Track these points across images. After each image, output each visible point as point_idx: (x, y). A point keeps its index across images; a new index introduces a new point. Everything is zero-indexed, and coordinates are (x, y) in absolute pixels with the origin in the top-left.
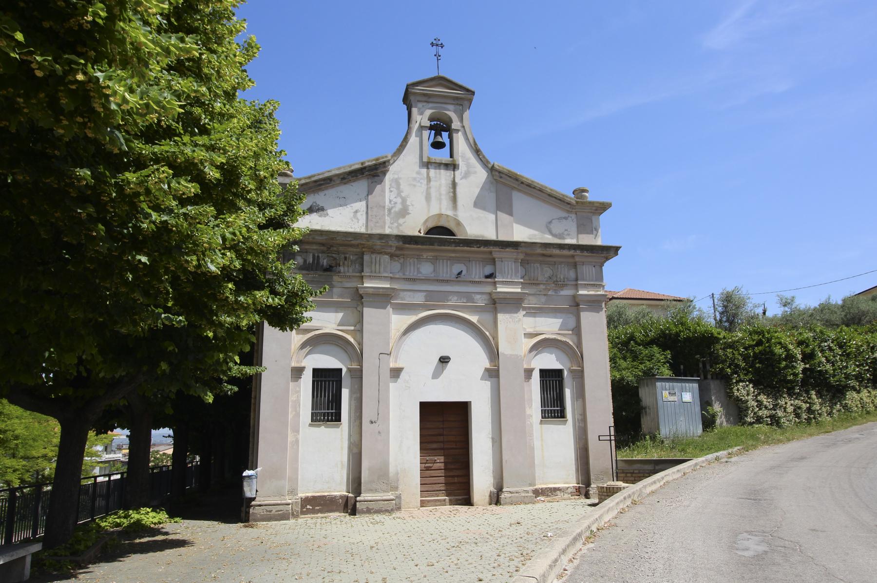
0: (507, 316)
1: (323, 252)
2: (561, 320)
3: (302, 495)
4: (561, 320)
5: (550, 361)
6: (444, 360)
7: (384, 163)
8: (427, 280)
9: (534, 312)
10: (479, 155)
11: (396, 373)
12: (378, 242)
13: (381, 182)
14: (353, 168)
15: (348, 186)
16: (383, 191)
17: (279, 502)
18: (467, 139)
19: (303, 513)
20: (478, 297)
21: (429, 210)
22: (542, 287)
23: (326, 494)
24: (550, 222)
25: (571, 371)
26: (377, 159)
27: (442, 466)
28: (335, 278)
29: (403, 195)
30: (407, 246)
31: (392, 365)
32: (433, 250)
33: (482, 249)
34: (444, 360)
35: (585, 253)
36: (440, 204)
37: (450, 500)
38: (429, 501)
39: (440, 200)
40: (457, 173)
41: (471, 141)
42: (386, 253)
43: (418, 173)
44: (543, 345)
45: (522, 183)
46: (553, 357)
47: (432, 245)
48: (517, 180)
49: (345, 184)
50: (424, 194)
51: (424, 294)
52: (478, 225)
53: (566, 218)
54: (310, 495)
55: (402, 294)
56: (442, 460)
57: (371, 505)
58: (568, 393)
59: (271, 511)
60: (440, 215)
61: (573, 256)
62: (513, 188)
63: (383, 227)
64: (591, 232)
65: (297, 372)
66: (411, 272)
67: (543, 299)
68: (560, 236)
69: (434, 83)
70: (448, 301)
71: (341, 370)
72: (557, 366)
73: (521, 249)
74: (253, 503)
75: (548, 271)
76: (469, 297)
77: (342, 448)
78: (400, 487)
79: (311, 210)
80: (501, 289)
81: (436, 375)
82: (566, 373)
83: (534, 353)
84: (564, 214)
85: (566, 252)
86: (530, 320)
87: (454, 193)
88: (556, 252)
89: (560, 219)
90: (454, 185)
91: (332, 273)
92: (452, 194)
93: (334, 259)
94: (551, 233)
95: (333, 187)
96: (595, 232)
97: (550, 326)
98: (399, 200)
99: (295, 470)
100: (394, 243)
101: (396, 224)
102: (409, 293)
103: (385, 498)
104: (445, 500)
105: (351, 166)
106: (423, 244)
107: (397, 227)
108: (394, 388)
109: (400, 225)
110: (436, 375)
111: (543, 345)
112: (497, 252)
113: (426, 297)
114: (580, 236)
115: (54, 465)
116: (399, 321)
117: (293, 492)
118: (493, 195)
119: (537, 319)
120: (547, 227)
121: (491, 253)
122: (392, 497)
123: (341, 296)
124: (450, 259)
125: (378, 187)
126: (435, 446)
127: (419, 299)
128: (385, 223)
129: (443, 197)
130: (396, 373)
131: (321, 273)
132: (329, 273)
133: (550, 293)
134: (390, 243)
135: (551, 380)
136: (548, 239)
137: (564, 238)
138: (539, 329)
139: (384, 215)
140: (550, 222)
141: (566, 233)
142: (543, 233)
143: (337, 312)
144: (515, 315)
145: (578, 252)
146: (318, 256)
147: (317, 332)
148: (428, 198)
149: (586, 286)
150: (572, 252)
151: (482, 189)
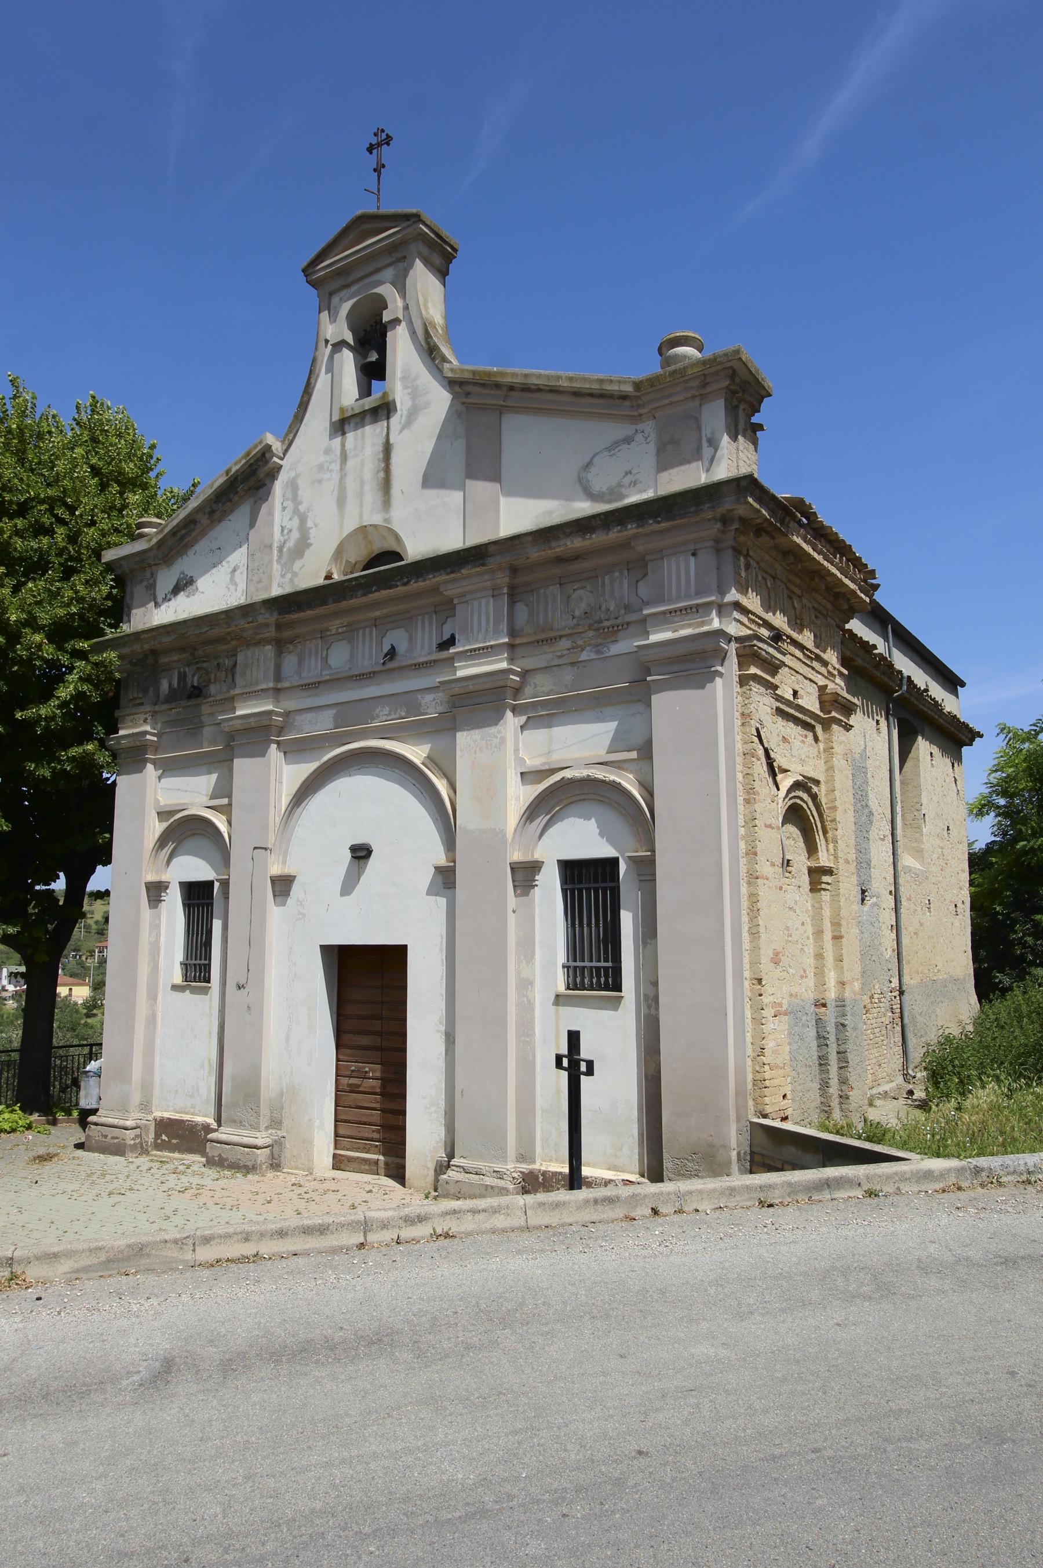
0: (476, 734)
1: (189, 664)
2: (613, 725)
3: (158, 1114)
4: (613, 725)
5: (582, 837)
6: (361, 853)
7: (263, 454)
8: (337, 681)
9: (543, 715)
10: (433, 359)
11: (283, 885)
12: (242, 623)
13: (266, 496)
14: (215, 486)
15: (225, 524)
16: (271, 514)
17: (115, 1122)
18: (413, 333)
19: (158, 1147)
20: (429, 697)
21: (341, 527)
22: (565, 644)
23: (186, 1117)
24: (589, 465)
25: (633, 861)
26: (248, 454)
27: (376, 1084)
28: (206, 709)
29: (302, 508)
30: (294, 616)
31: (276, 870)
32: (337, 614)
33: (416, 585)
34: (361, 853)
35: (652, 526)
36: (361, 505)
37: (386, 1164)
38: (350, 1159)
39: (361, 494)
40: (395, 420)
41: (420, 333)
42: (268, 641)
43: (328, 451)
44: (557, 797)
45: (511, 388)
46: (591, 826)
47: (324, 603)
48: (497, 386)
49: (220, 521)
50: (336, 493)
51: (331, 712)
52: (432, 525)
53: (628, 440)
54: (166, 1115)
55: (299, 719)
56: (378, 1074)
57: (226, 1151)
58: (627, 920)
59: (106, 1136)
60: (363, 530)
61: (626, 545)
62: (501, 410)
63: (269, 588)
64: (696, 455)
65: (525, 874)
66: (313, 670)
67: (568, 675)
68: (615, 493)
69: (351, 237)
70: (373, 719)
71: (614, 862)
72: (604, 850)
73: (493, 562)
74: (91, 1119)
75: (583, 599)
76: (409, 701)
77: (210, 1033)
78: (285, 1123)
79: (176, 590)
80: (466, 670)
81: (348, 886)
82: (623, 867)
83: (541, 821)
84: (624, 430)
85: (599, 538)
86: (538, 736)
87: (387, 470)
88: (577, 543)
89: (612, 448)
90: (387, 449)
91: (199, 700)
92: (382, 475)
93: (193, 674)
94: (590, 495)
95: (203, 533)
96: (707, 452)
97: (581, 745)
98: (296, 521)
99: (149, 1067)
100: (271, 618)
101: (289, 576)
102: (309, 716)
103: (246, 1140)
104: (377, 1162)
105: (211, 486)
106: (311, 607)
107: (291, 581)
108: (276, 915)
109: (295, 574)
110: (348, 886)
111: (557, 797)
112: (450, 585)
113: (336, 717)
114: (664, 476)
115: (21, 1032)
116: (287, 774)
117: (145, 1106)
118: (461, 444)
119: (556, 731)
120: (580, 480)
121: (435, 590)
122: (260, 1142)
123: (213, 743)
124: (375, 623)
125: (265, 507)
126: (366, 1040)
127: (321, 724)
128: (270, 578)
129: (367, 487)
130: (283, 885)
131: (184, 703)
132: (193, 702)
133: (584, 656)
134: (261, 619)
135: (589, 885)
136: (584, 508)
137: (622, 497)
138: (558, 758)
139: (271, 562)
140: (589, 465)
141: (627, 480)
142: (569, 499)
143: (210, 773)
144: (493, 730)
145: (632, 529)
146: (185, 673)
147: (177, 817)
148: (341, 502)
149: (665, 619)
150: (614, 535)
151: (439, 438)
